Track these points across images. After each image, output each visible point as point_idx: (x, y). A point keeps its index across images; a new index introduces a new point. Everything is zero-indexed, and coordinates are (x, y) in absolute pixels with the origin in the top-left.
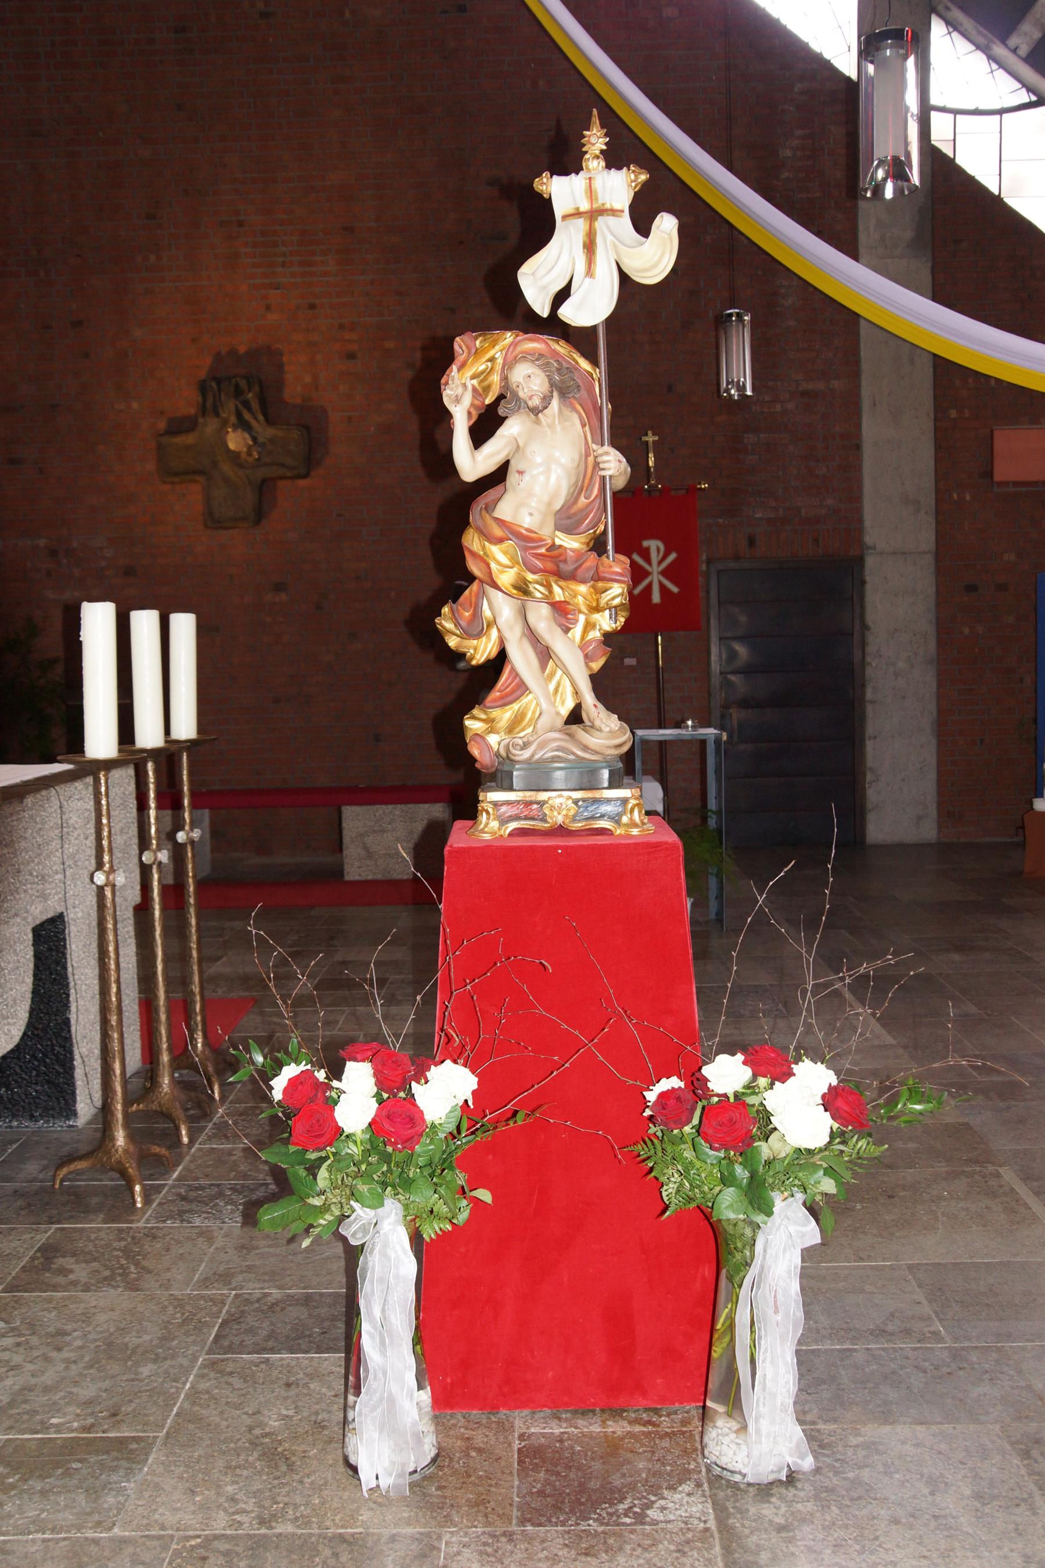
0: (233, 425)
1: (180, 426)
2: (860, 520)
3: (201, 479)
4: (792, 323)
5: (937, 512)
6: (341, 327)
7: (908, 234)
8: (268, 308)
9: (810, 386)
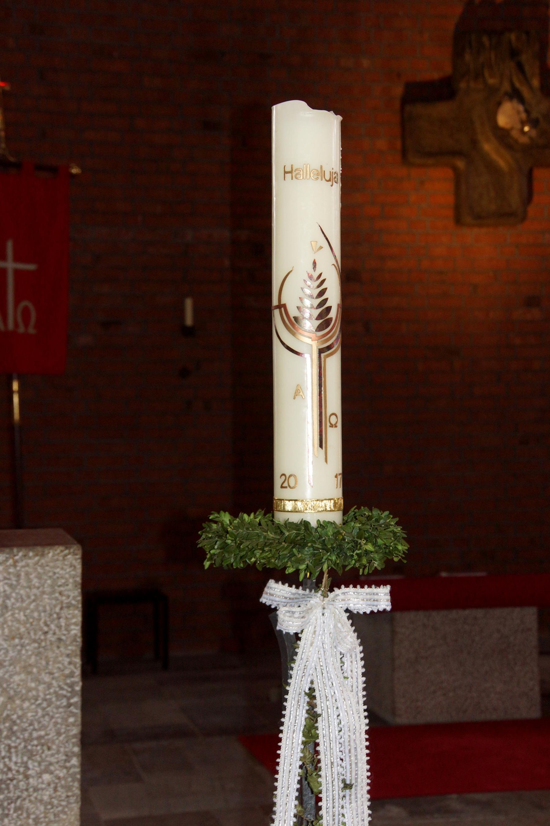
0: (506, 94)
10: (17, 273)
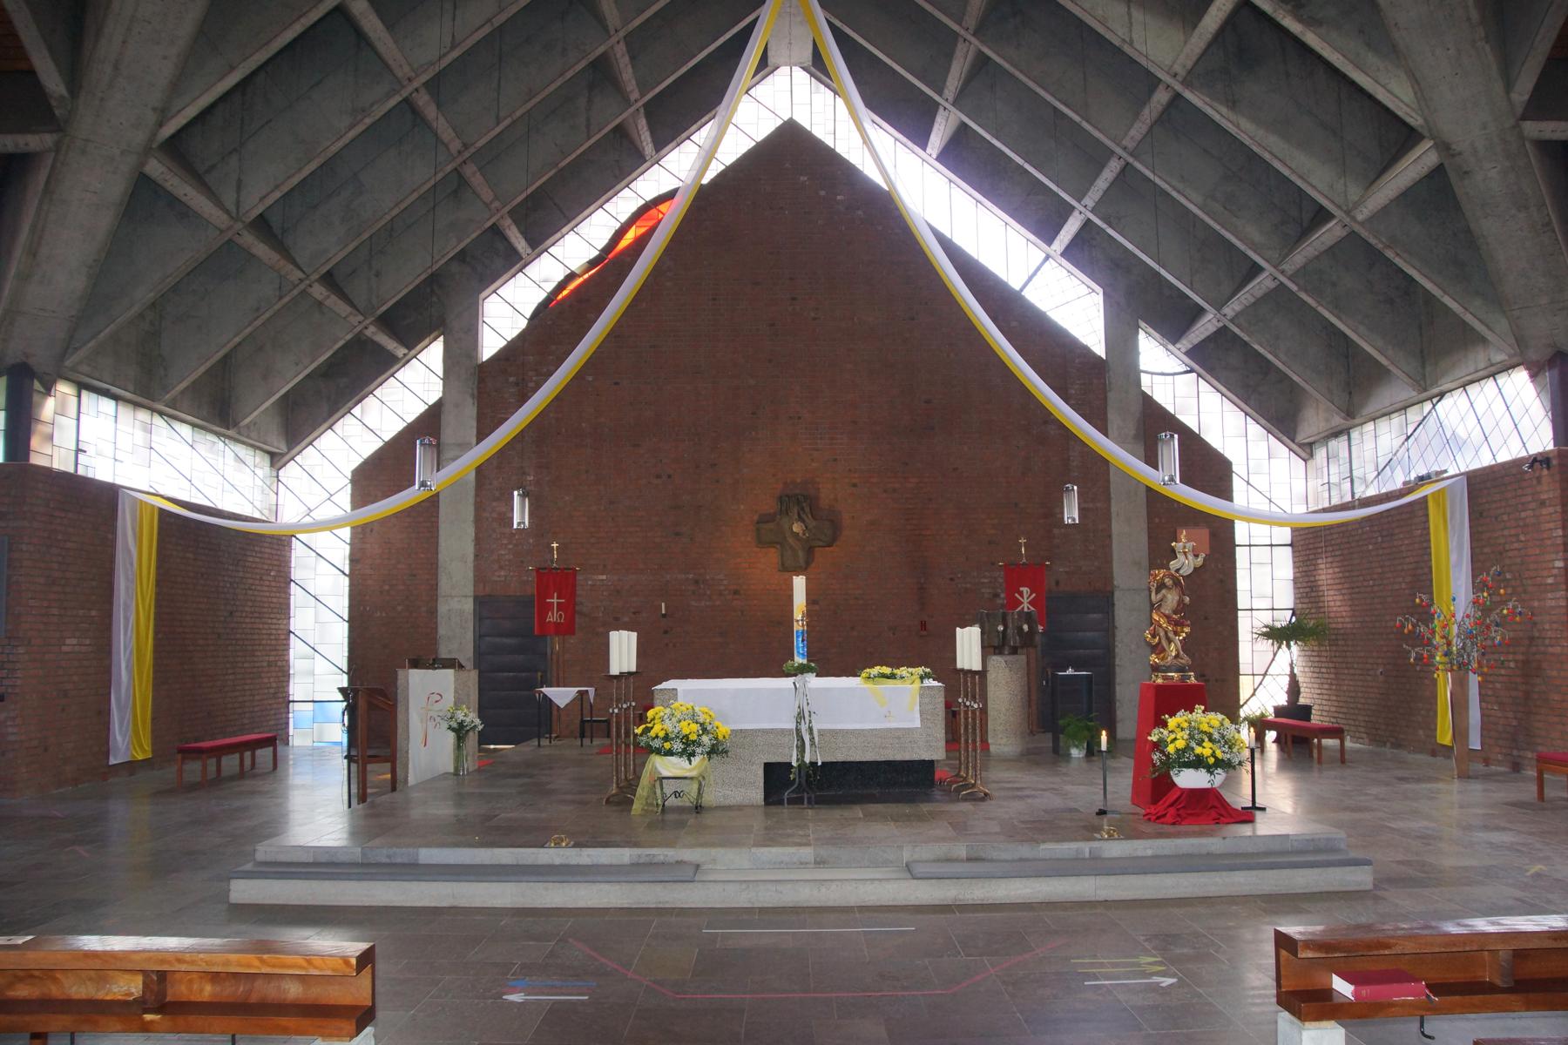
1: (765, 519)
7: (1133, 432)
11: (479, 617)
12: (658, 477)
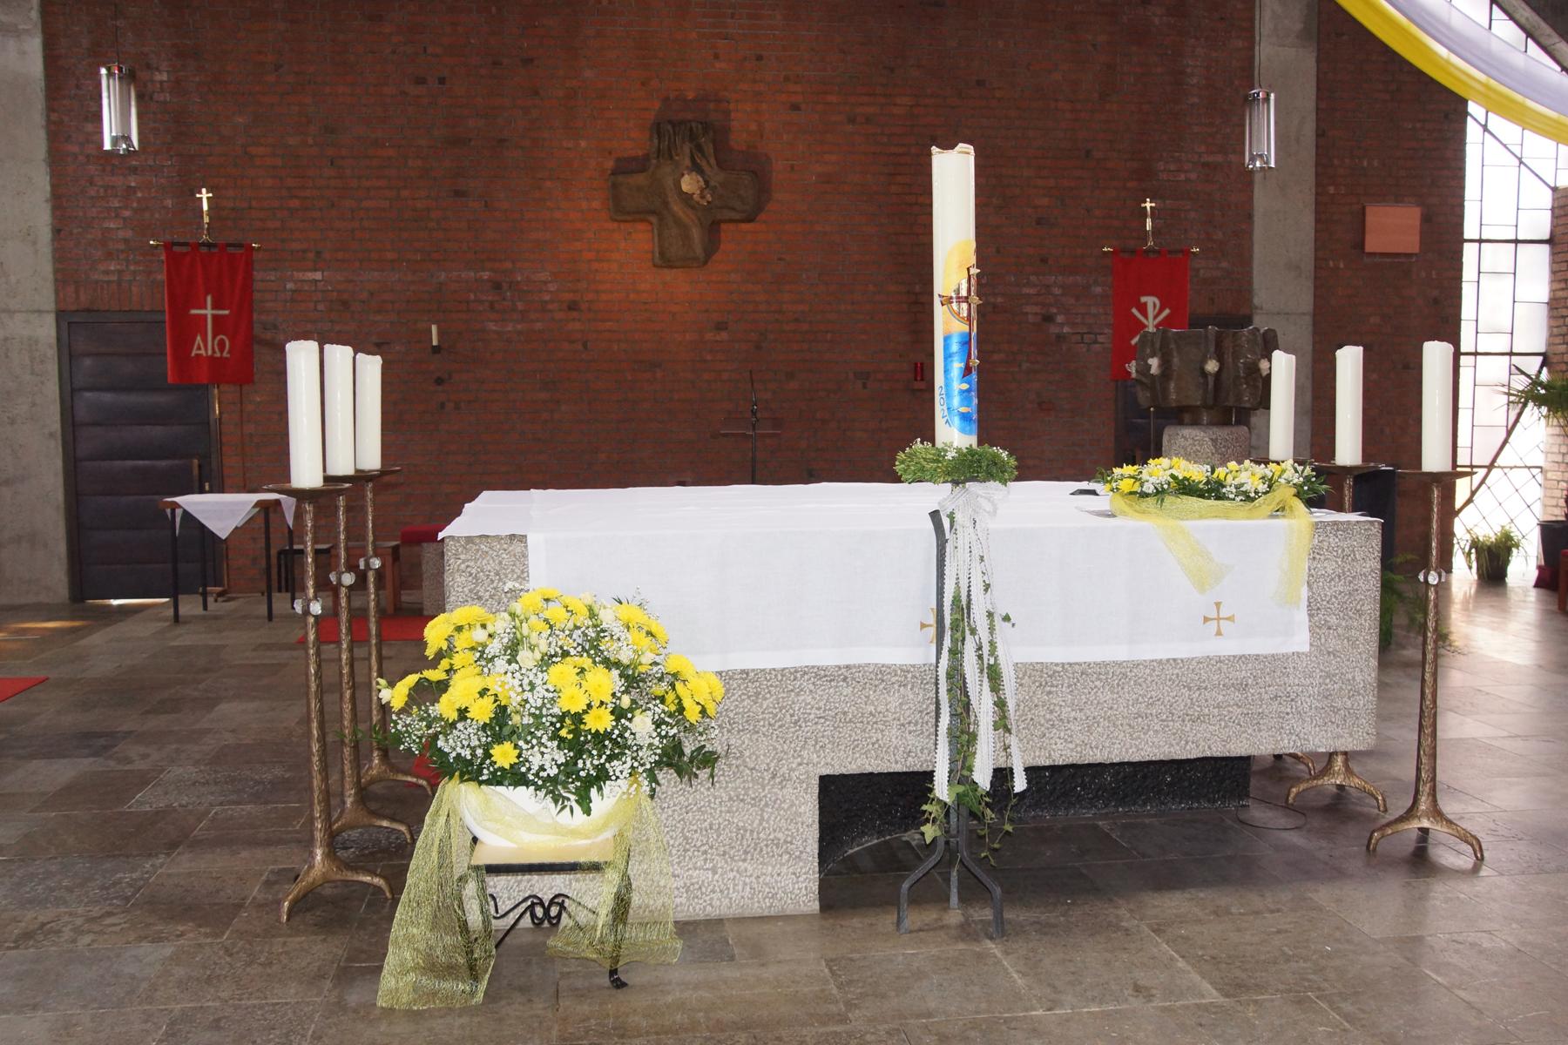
1: (625, 167)
2: (1250, 283)
3: (654, 219)
4: (1196, 100)
5: (1316, 278)
6: (787, 79)
7: (1299, 26)
8: (716, 57)
9: (1210, 159)
10: (215, 317)
11: (68, 354)
12: (421, 81)
